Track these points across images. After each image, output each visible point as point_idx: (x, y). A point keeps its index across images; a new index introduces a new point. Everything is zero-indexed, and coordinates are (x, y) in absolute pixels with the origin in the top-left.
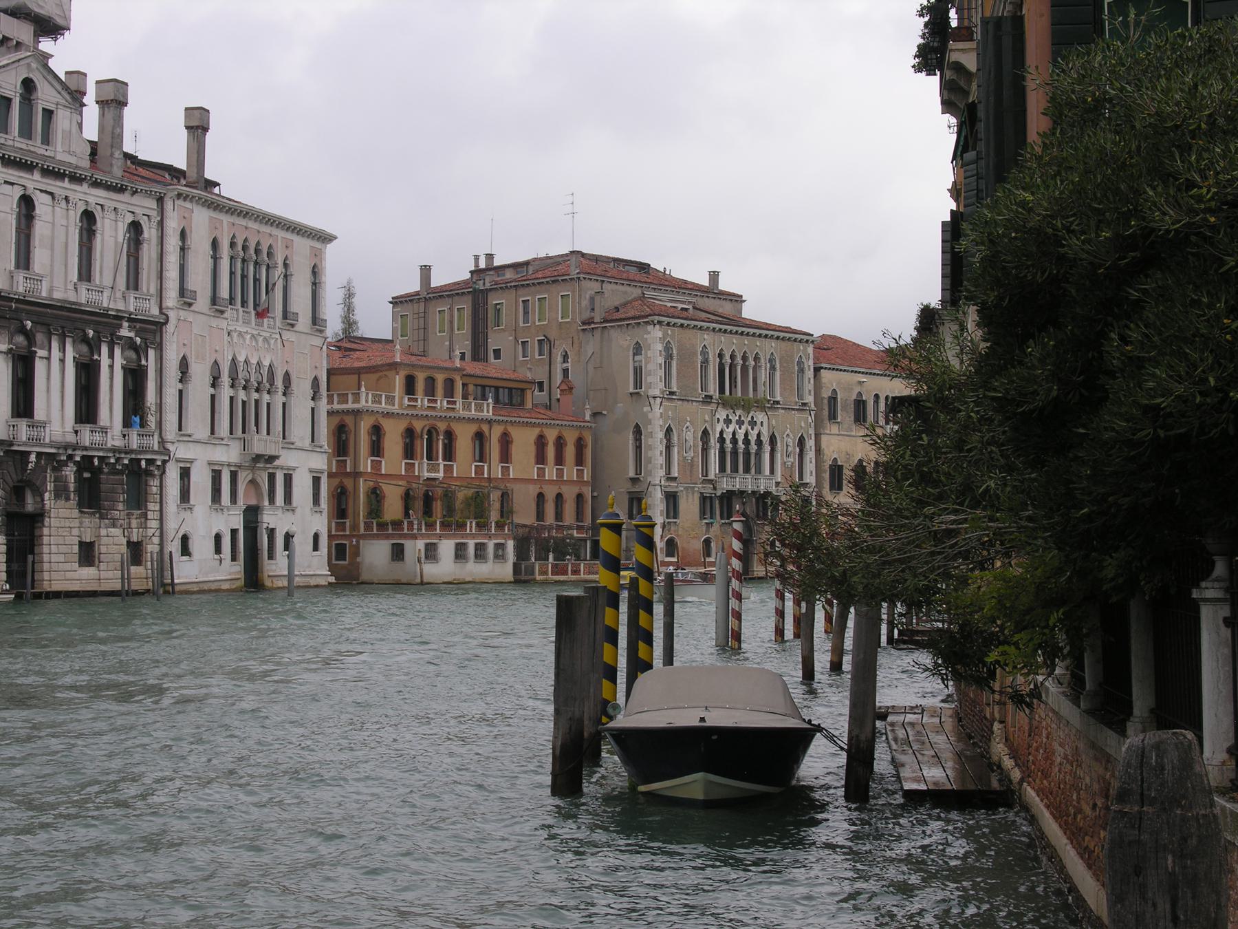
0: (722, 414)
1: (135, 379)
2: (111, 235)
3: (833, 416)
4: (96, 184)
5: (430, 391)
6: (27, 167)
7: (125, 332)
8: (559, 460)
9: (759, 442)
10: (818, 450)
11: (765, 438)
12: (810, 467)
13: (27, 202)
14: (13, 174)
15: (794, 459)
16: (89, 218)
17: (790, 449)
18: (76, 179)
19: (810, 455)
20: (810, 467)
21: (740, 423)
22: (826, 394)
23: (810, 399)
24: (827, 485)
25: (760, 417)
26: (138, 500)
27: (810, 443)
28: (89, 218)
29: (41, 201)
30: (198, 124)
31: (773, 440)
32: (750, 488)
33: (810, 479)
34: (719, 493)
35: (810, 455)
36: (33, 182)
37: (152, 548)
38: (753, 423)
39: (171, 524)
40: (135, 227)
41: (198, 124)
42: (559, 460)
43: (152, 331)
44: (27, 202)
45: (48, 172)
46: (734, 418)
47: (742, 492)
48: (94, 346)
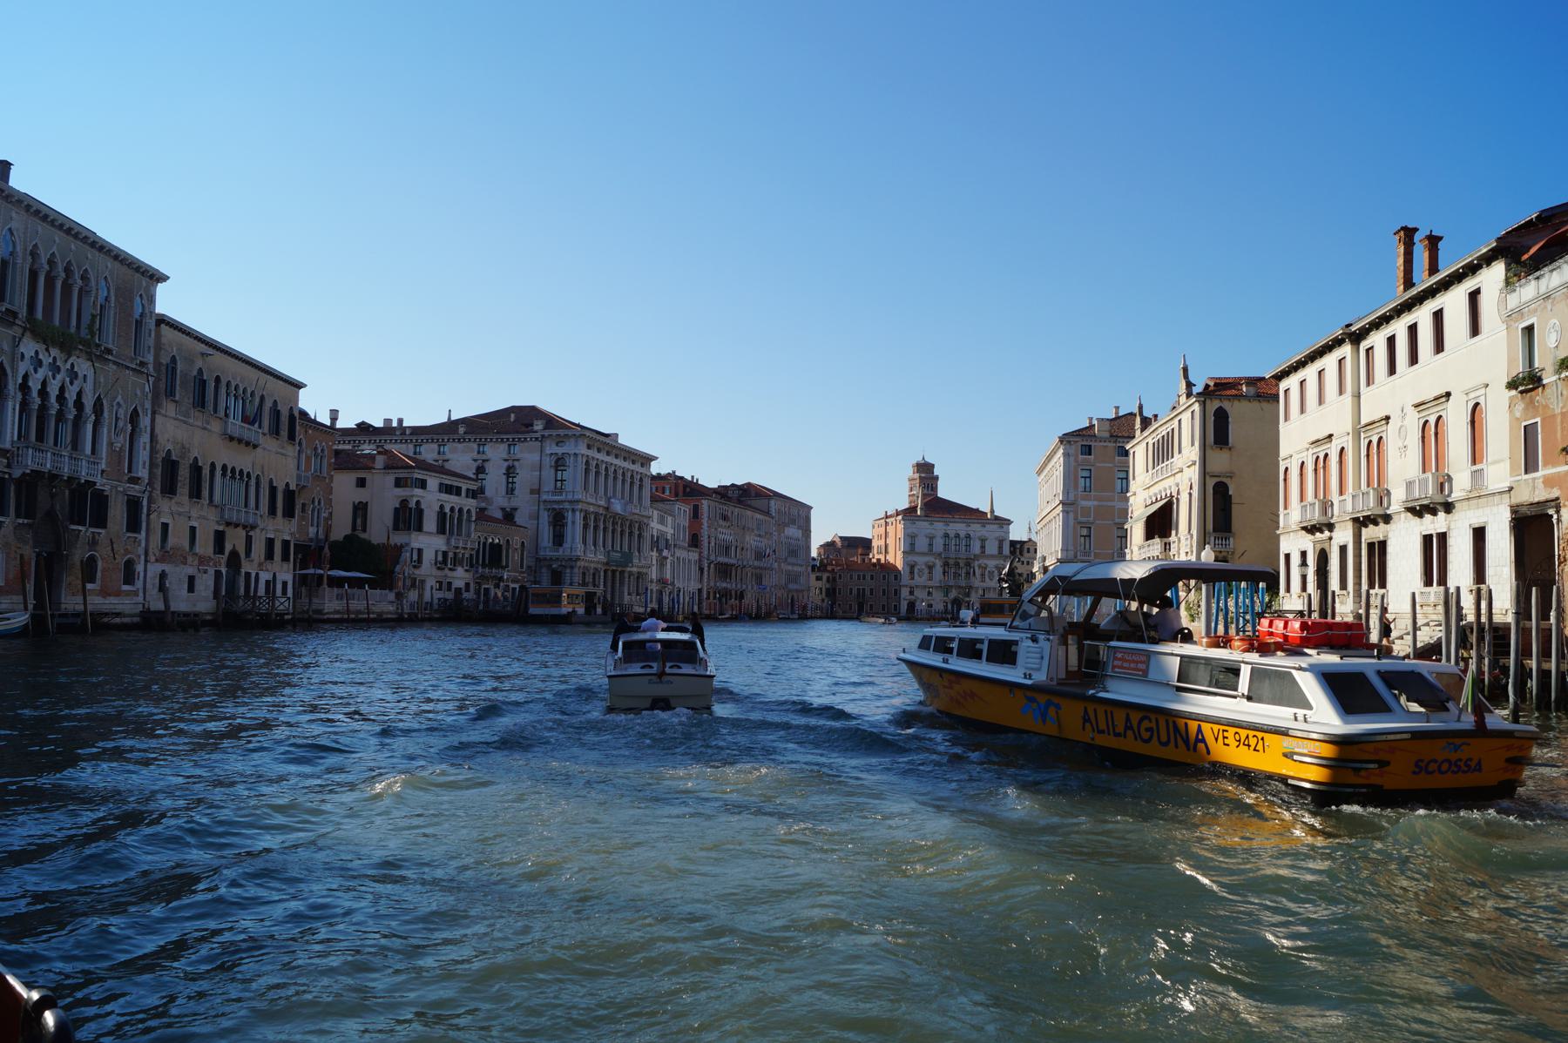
3: (170, 393)
9: (79, 404)
10: (153, 437)
11: (88, 402)
12: (143, 455)
15: (122, 441)
17: (121, 424)
19: (145, 439)
20: (143, 455)
21: (56, 369)
22: (165, 360)
23: (150, 358)
24: (158, 485)
25: (83, 367)
27: (145, 421)
31: (98, 408)
32: (66, 471)
33: (143, 473)
34: (17, 473)
35: (145, 439)
38: (73, 375)
46: (46, 360)
47: (54, 477)
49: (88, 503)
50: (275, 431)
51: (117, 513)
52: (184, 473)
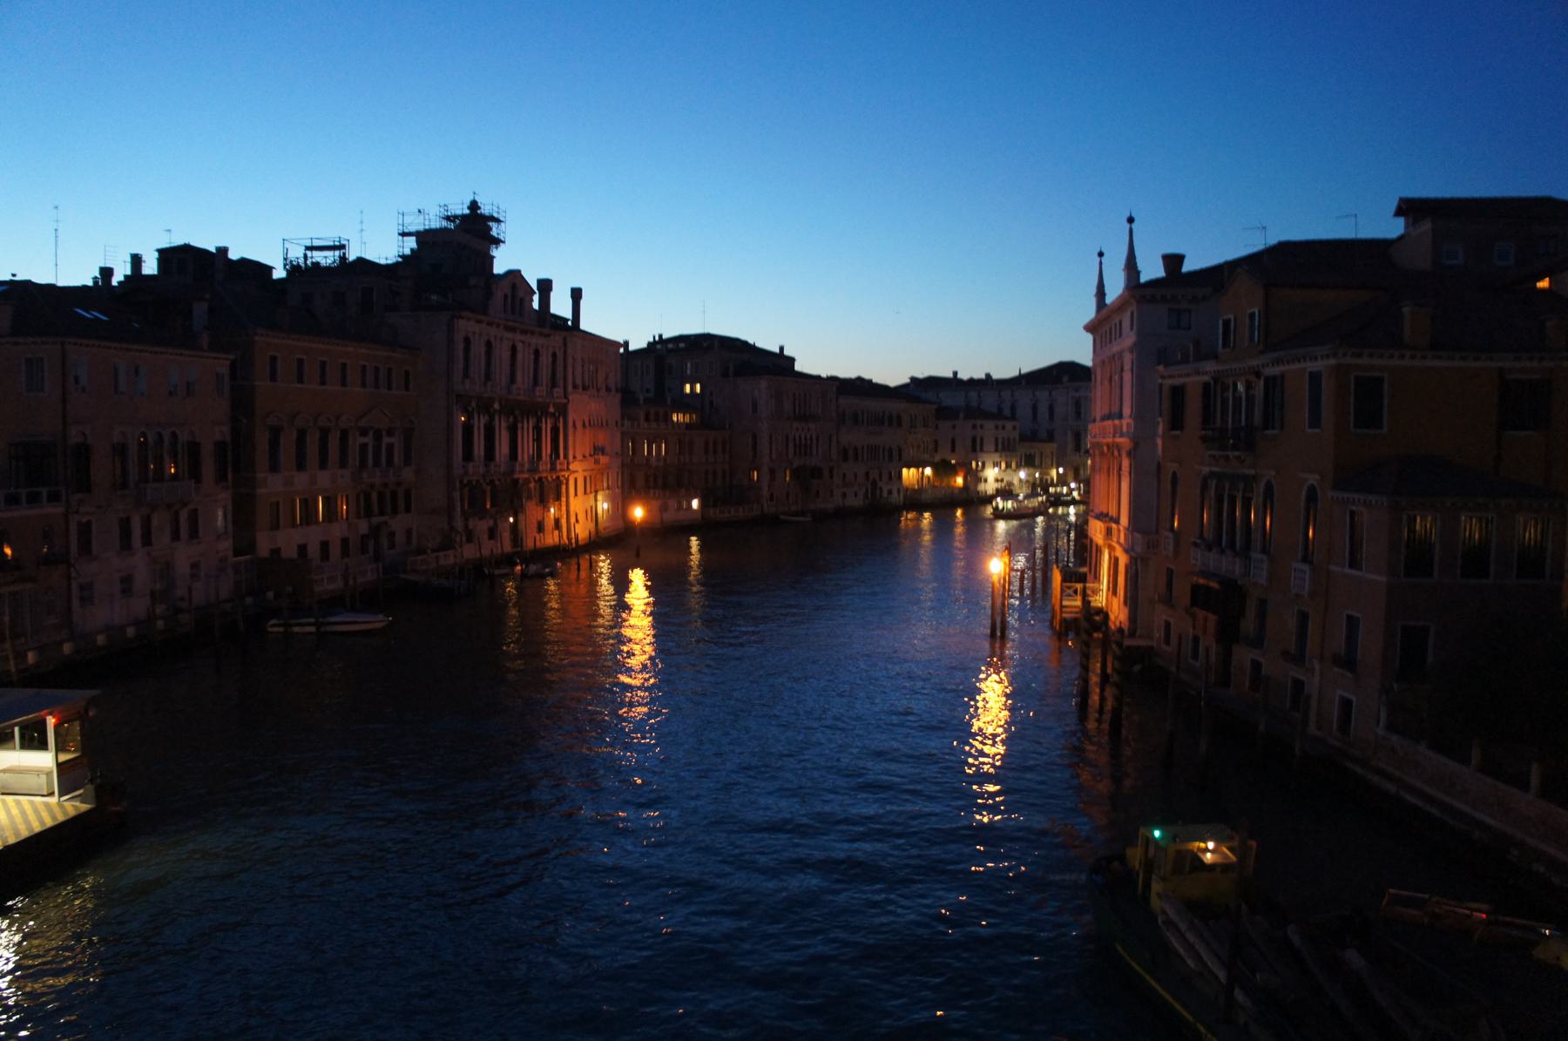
0: (795, 425)
1: (555, 430)
2: (545, 360)
4: (541, 334)
5: (657, 420)
6: (513, 330)
7: (552, 410)
8: (715, 452)
13: (514, 349)
14: (509, 335)
16: (537, 353)
18: (533, 333)
25: (812, 426)
26: (558, 498)
28: (537, 353)
29: (520, 346)
30: (576, 294)
36: (518, 337)
37: (564, 522)
39: (572, 508)
40: (554, 355)
41: (576, 294)
42: (715, 452)
43: (563, 410)
44: (514, 349)
45: (524, 332)
48: (539, 421)
49: (816, 473)
50: (890, 424)
51: (826, 473)
52: (851, 453)
